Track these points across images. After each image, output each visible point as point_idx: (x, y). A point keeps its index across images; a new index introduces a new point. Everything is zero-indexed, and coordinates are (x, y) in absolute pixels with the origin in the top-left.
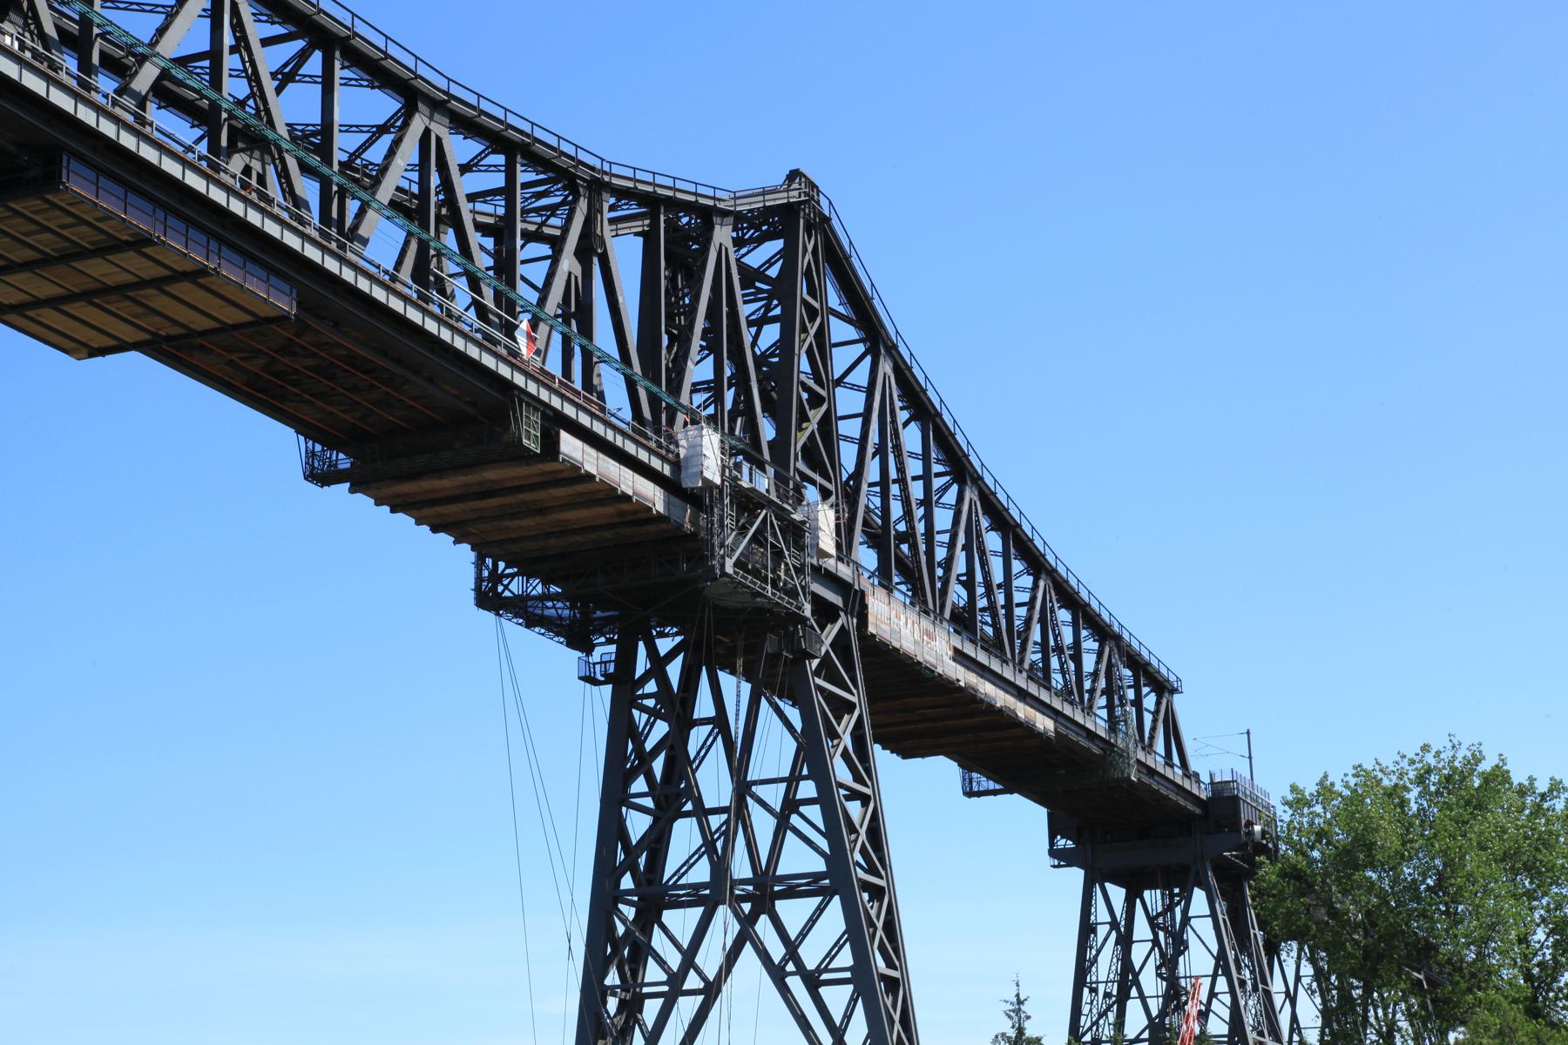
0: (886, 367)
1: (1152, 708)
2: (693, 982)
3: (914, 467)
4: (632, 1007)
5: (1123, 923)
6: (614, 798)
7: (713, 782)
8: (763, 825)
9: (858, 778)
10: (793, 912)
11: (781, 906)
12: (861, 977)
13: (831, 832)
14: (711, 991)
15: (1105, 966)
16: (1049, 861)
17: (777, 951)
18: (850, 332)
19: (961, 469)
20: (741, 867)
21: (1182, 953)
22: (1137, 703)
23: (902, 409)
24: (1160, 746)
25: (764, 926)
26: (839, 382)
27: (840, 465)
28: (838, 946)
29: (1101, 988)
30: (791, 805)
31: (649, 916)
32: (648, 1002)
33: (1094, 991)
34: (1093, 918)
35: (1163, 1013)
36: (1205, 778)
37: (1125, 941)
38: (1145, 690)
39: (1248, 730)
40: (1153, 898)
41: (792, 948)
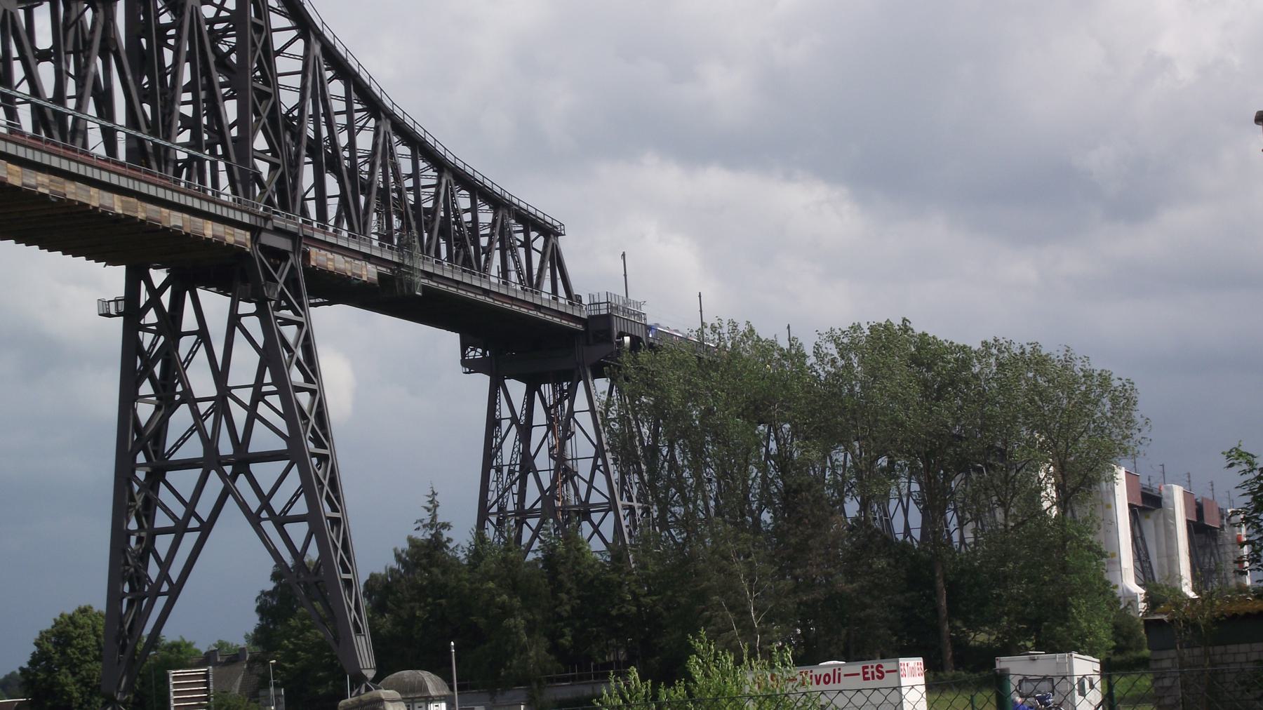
0: (317, 48)
2: (194, 523)
3: (338, 106)
6: (128, 397)
7: (201, 381)
8: (240, 416)
10: (266, 473)
11: (255, 468)
12: (313, 517)
14: (206, 529)
16: (460, 368)
17: (254, 504)
18: (286, 23)
20: (225, 447)
21: (570, 437)
22: (527, 245)
23: (327, 70)
24: (547, 286)
25: (242, 483)
27: (280, 102)
28: (297, 495)
30: (258, 396)
31: (157, 476)
32: (159, 538)
34: (497, 413)
35: (554, 486)
36: (585, 301)
37: (525, 432)
38: (533, 235)
39: (624, 253)
41: (265, 500)
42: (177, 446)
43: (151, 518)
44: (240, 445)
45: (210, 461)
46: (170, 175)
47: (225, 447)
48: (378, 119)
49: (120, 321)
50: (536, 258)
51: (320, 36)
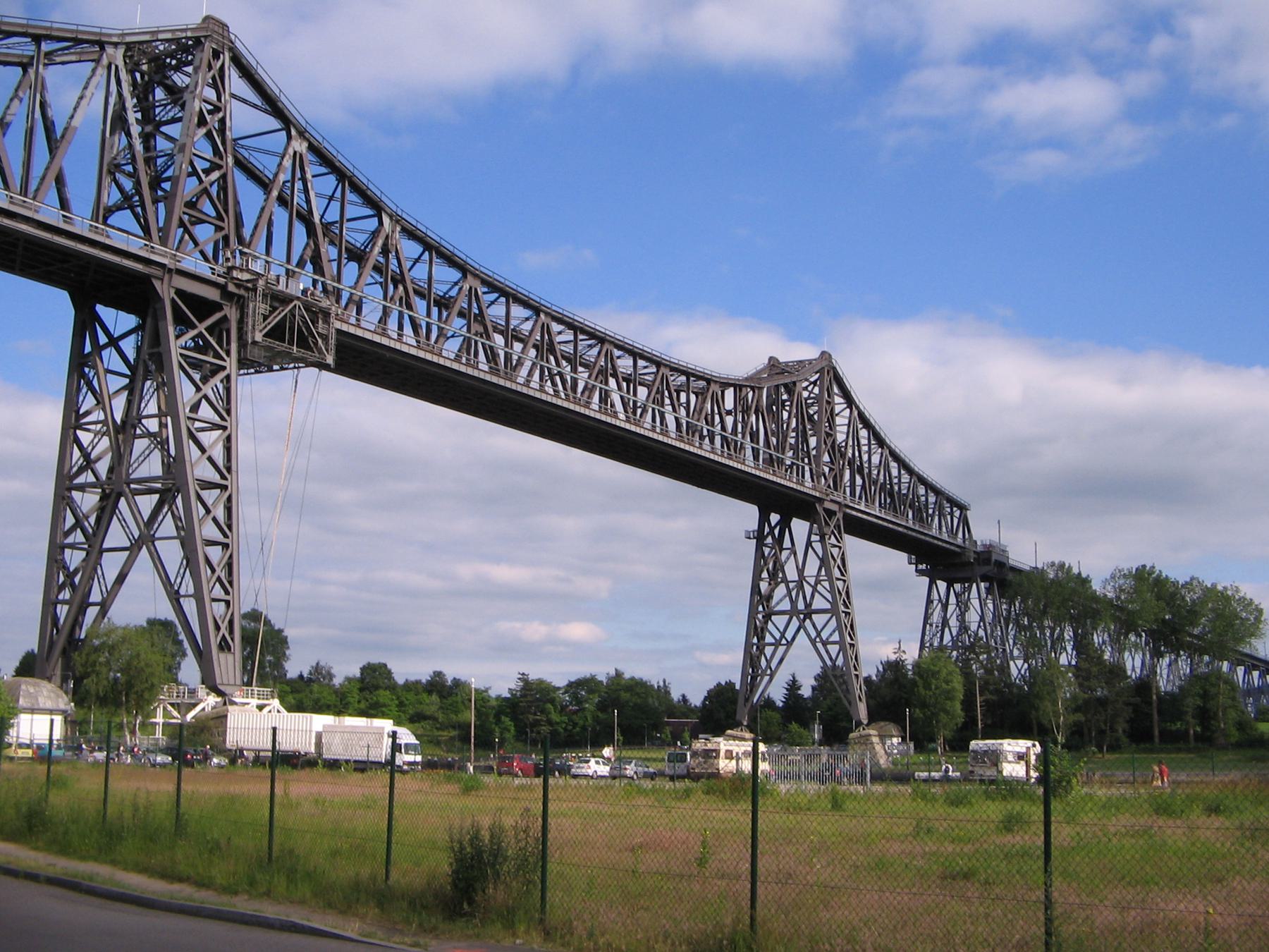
0: (856, 413)
1: (958, 516)
2: (784, 641)
3: (864, 441)
4: (761, 650)
7: (791, 573)
8: (808, 590)
9: (842, 575)
11: (814, 616)
12: (841, 643)
13: (832, 591)
14: (789, 644)
15: (936, 617)
17: (813, 634)
18: (842, 400)
19: (881, 443)
20: (801, 606)
22: (952, 514)
24: (960, 535)
26: (837, 415)
28: (834, 631)
30: (818, 582)
31: (768, 617)
32: (767, 648)
35: (959, 634)
36: (979, 543)
37: (945, 607)
38: (955, 509)
40: (957, 587)
41: (819, 634)
42: (778, 604)
43: (763, 638)
44: (808, 605)
45: (793, 612)
46: (783, 471)
47: (801, 606)
48: (883, 448)
49: (755, 540)
50: (956, 521)
51: (857, 408)
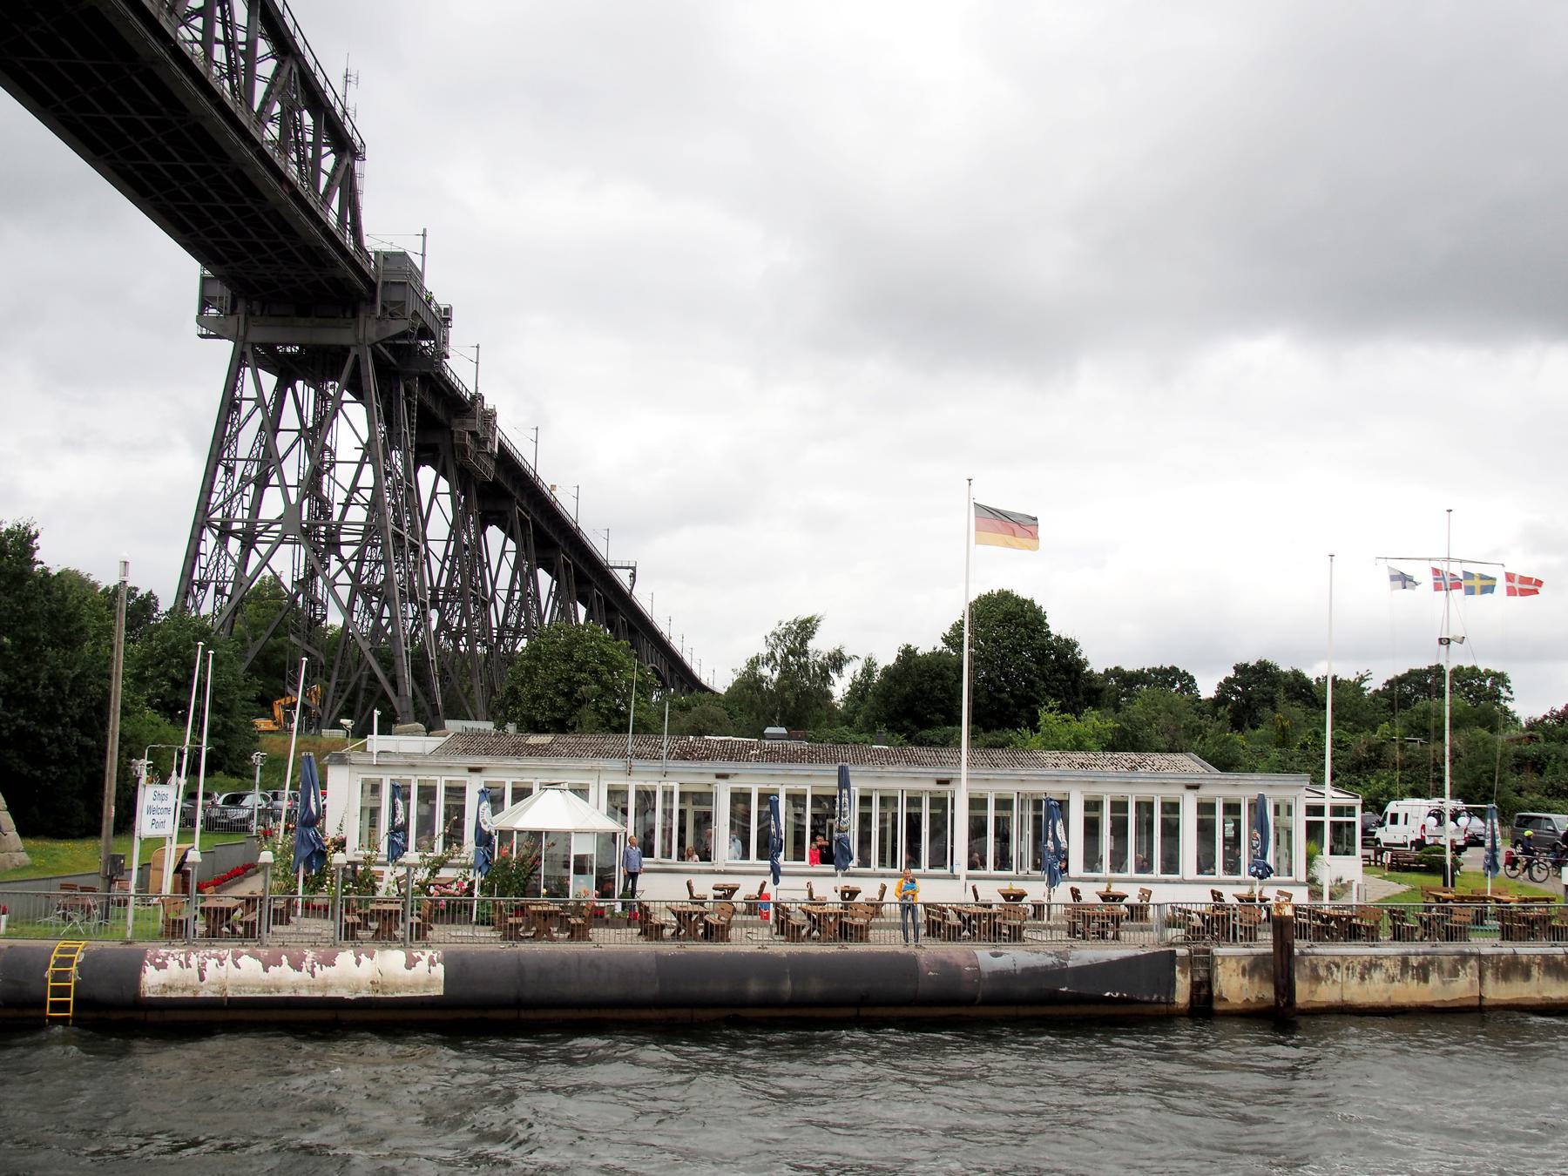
5: (271, 408)
15: (247, 440)
29: (240, 466)
33: (230, 471)
34: (238, 393)
